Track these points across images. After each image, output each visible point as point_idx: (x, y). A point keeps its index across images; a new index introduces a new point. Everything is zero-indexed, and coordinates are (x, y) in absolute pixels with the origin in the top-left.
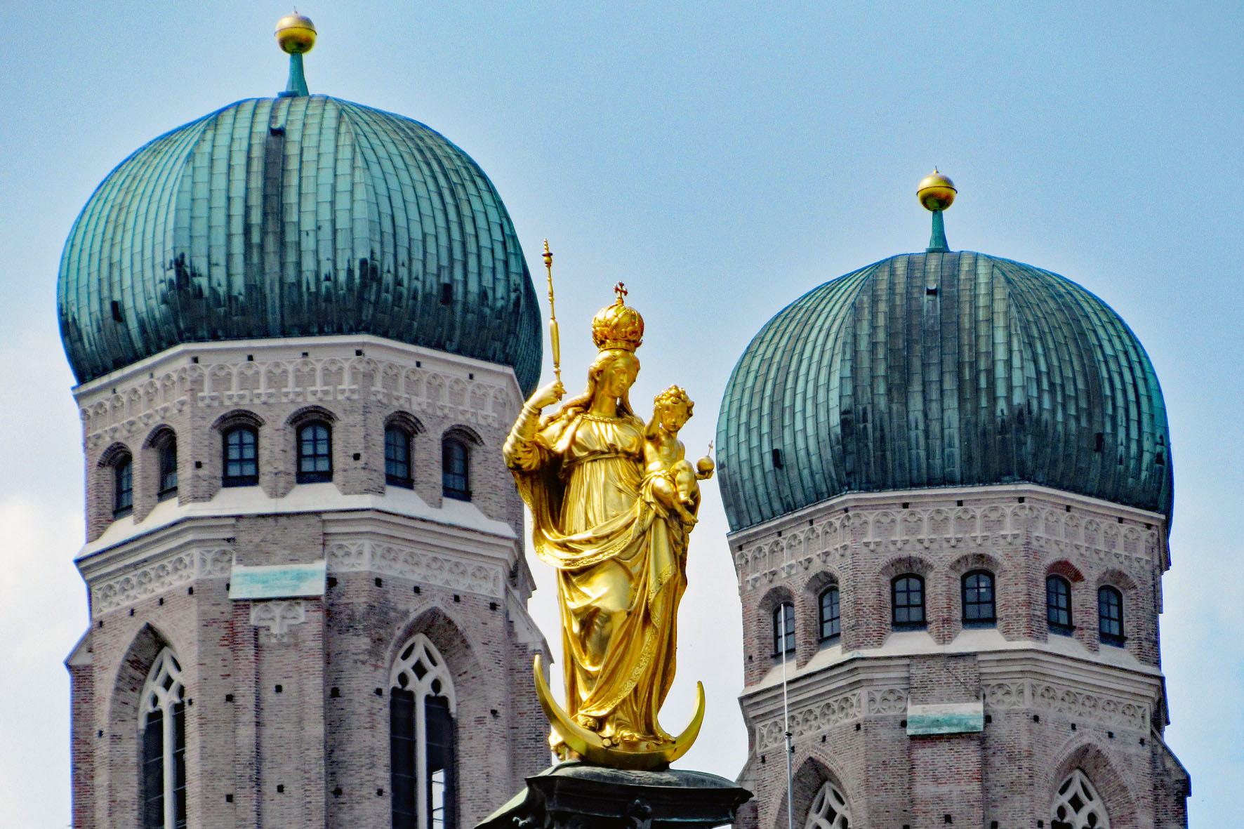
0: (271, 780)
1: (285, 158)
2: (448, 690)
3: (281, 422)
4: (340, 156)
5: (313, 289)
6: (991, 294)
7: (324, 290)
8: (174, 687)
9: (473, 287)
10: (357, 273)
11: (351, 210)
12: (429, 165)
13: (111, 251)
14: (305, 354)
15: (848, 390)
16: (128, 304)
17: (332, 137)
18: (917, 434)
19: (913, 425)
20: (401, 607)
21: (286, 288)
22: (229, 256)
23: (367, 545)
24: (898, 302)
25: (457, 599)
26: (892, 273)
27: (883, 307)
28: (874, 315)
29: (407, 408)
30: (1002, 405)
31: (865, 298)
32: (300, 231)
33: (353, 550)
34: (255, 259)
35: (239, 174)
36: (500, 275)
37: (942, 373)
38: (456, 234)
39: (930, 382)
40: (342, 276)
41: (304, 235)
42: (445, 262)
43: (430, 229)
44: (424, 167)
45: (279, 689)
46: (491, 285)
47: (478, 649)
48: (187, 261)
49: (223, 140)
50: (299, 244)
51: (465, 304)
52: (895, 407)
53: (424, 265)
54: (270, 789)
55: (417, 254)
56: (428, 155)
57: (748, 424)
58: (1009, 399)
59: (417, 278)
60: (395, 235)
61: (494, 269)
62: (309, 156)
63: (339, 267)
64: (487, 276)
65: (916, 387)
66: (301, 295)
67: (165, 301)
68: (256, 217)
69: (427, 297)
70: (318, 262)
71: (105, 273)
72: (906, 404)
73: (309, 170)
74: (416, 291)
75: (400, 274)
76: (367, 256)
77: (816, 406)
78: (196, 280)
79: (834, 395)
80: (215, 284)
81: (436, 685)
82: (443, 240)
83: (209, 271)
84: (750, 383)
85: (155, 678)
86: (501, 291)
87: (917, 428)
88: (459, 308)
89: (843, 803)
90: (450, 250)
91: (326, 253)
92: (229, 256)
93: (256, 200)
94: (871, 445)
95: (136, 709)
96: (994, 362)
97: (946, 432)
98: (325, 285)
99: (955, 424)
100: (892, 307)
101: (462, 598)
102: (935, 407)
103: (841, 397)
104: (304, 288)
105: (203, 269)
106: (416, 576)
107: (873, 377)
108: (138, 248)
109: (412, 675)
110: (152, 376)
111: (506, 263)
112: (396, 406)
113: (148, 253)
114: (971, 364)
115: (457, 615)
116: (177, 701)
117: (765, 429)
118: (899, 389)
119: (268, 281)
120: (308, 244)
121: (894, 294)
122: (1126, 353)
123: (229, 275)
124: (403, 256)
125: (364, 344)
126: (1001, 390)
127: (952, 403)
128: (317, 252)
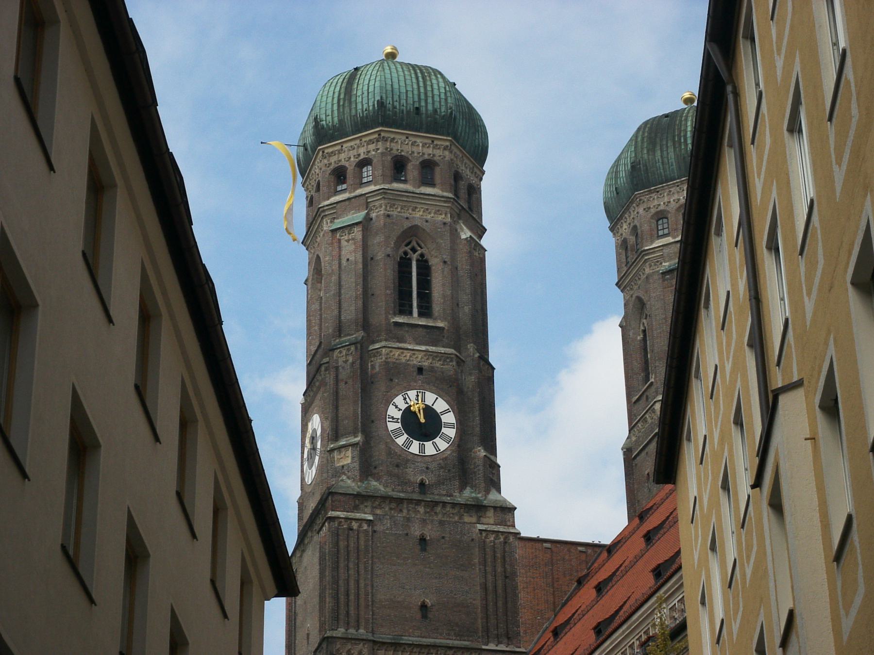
5: (361, 115)
9: (430, 107)
10: (376, 106)
15: (633, 155)
21: (352, 118)
22: (332, 111)
34: (341, 110)
36: (443, 104)
38: (422, 90)
39: (663, 145)
40: (371, 108)
42: (416, 99)
43: (409, 88)
45: (348, 260)
46: (439, 107)
48: (318, 117)
51: (426, 114)
52: (650, 157)
53: (407, 102)
55: (403, 97)
60: (392, 91)
61: (440, 102)
64: (437, 105)
65: (658, 148)
66: (357, 118)
68: (342, 96)
69: (408, 112)
70: (363, 105)
72: (654, 154)
73: (363, 77)
74: (403, 111)
76: (380, 98)
81: (422, 255)
82: (416, 92)
86: (443, 109)
87: (659, 162)
88: (424, 116)
92: (332, 111)
93: (343, 90)
94: (642, 172)
96: (686, 132)
102: (665, 153)
105: (324, 119)
107: (642, 149)
111: (446, 100)
119: (346, 116)
120: (359, 100)
123: (332, 118)
124: (396, 98)
125: (381, 130)
127: (671, 150)
128: (362, 102)
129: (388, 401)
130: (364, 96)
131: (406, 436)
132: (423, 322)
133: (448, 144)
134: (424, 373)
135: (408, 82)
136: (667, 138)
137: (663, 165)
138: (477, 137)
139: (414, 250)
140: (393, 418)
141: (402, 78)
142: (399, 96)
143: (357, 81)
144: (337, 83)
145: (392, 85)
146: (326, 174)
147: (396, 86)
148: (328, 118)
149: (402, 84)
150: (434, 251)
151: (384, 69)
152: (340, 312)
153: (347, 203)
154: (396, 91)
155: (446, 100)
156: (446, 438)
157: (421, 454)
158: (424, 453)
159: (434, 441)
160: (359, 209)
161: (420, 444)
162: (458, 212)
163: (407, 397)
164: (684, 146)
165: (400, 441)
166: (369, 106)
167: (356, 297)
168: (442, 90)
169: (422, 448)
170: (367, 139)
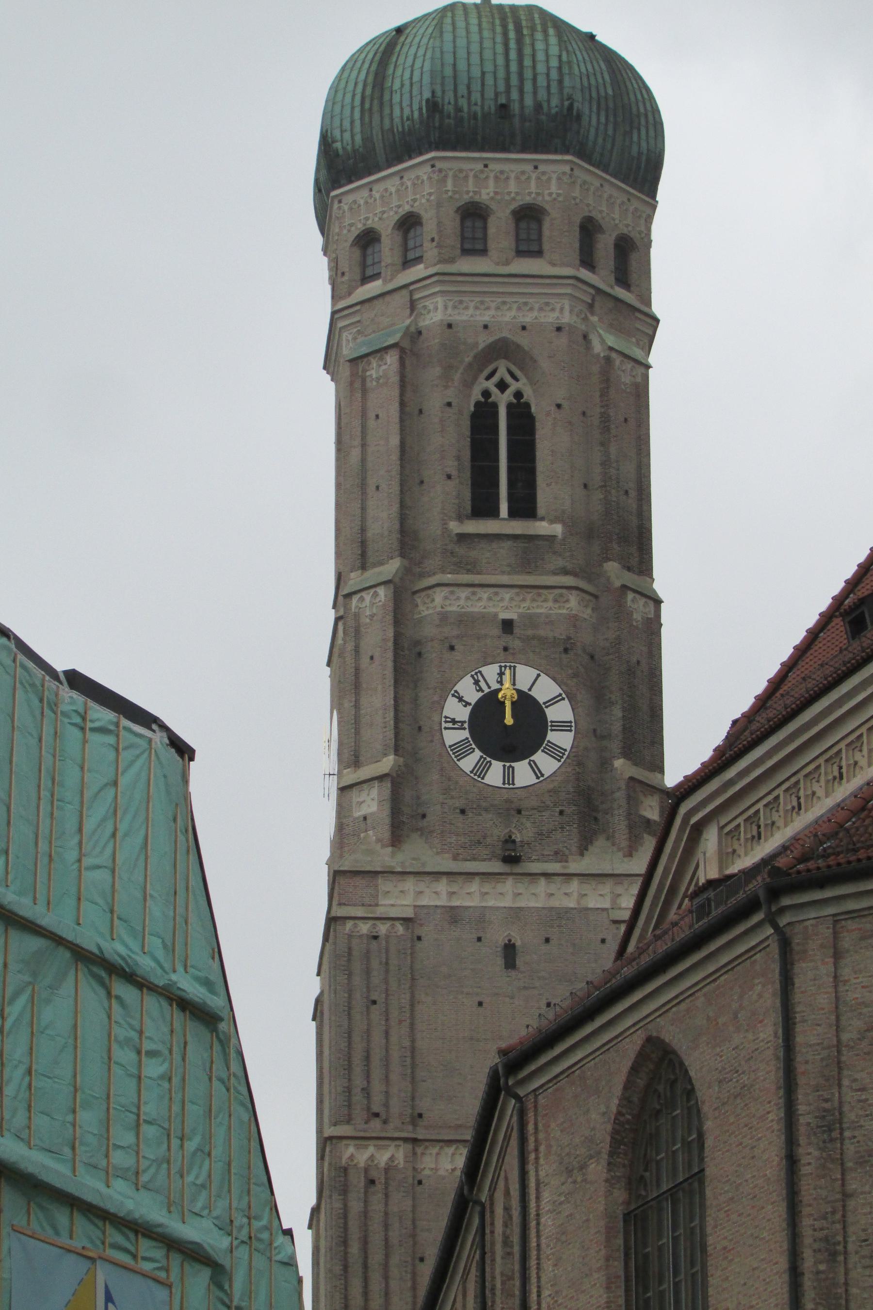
0: (372, 482)
2: (529, 394)
3: (389, 230)
5: (400, 129)
9: (529, 101)
12: (505, 27)
14: (402, 178)
20: (470, 341)
22: (352, 122)
23: (440, 300)
25: (524, 328)
29: (477, 198)
33: (431, 307)
34: (367, 119)
36: (554, 89)
38: (514, 67)
40: (416, 115)
42: (501, 88)
43: (489, 67)
45: (377, 416)
46: (545, 98)
47: (544, 364)
48: (329, 134)
50: (391, 100)
53: (482, 95)
54: (371, 489)
55: (476, 87)
59: (476, 104)
60: (455, 77)
61: (548, 87)
64: (542, 94)
68: (369, 91)
69: (486, 116)
70: (402, 109)
74: (475, 114)
75: (460, 104)
78: (335, 145)
81: (518, 395)
82: (501, 74)
83: (342, 136)
86: (555, 102)
90: (507, 79)
101: (528, 327)
105: (338, 137)
106: (486, 317)
109: (495, 391)
111: (560, 82)
112: (466, 198)
115: (523, 340)
119: (374, 132)
120: (396, 98)
123: (352, 136)
124: (462, 90)
125: (433, 159)
129: (446, 688)
131: (478, 754)
132: (518, 527)
133: (567, 168)
134: (516, 631)
135: (488, 54)
138: (635, 138)
139: (502, 386)
140: (454, 721)
141: (475, 48)
142: (468, 87)
143: (394, 59)
144: (363, 62)
145: (455, 65)
147: (462, 66)
149: (475, 59)
151: (441, 33)
154: (463, 79)
155: (560, 82)
156: (555, 752)
157: (507, 786)
158: (513, 784)
159: (532, 758)
161: (504, 766)
162: (590, 301)
163: (480, 678)
165: (468, 763)
166: (412, 111)
168: (554, 63)
169: (509, 776)
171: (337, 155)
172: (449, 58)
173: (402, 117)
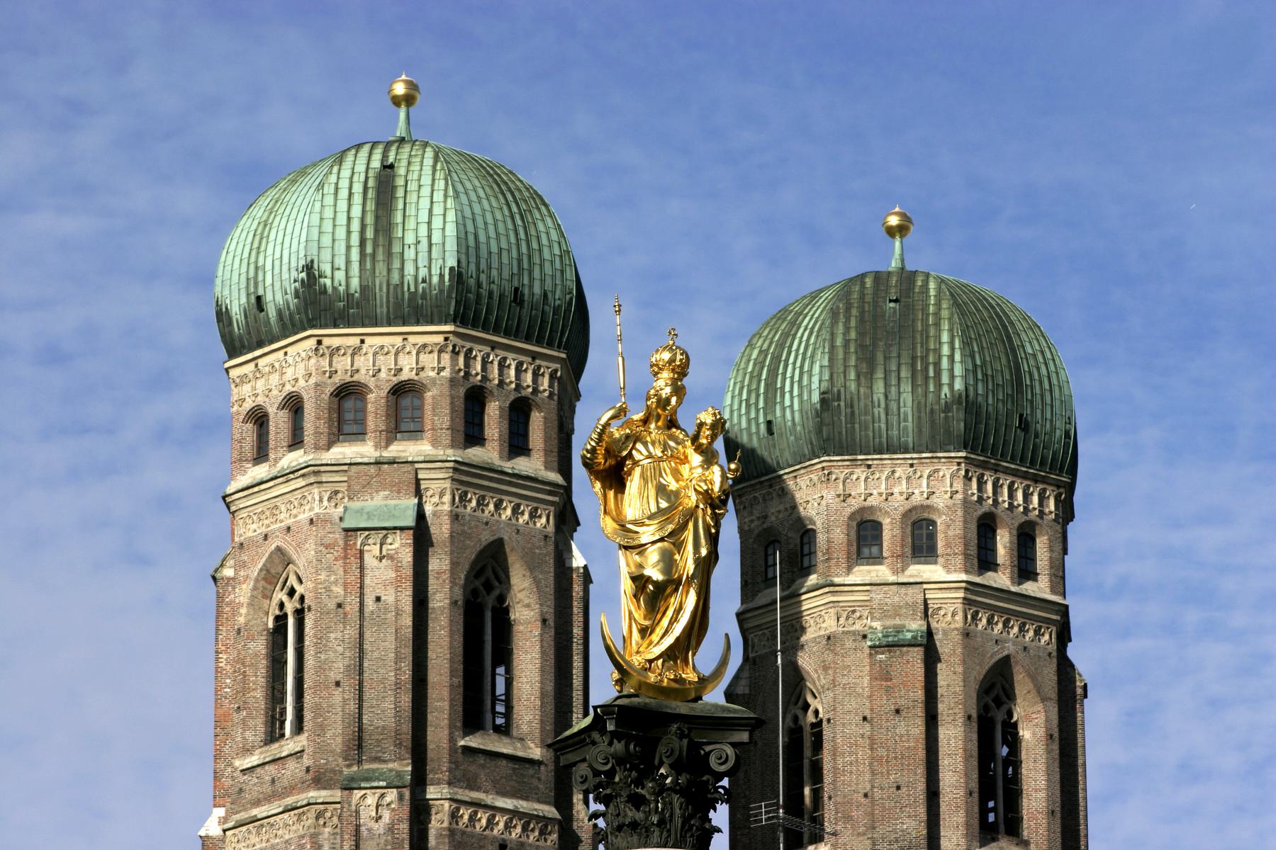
1: (394, 188)
4: (436, 188)
5: (412, 289)
6: (938, 304)
7: (421, 290)
8: (297, 596)
9: (537, 290)
10: (447, 277)
11: (443, 229)
12: (504, 195)
13: (257, 258)
15: (826, 376)
16: (269, 297)
17: (430, 172)
18: (880, 411)
19: (876, 404)
21: (392, 288)
22: (348, 262)
24: (867, 309)
26: (863, 284)
27: (854, 312)
28: (848, 319)
30: (945, 390)
31: (841, 306)
32: (403, 245)
34: (368, 266)
35: (358, 199)
37: (899, 365)
38: (524, 249)
39: (890, 371)
40: (435, 280)
41: (406, 247)
43: (504, 245)
44: (500, 196)
45: (378, 599)
48: (316, 266)
49: (346, 173)
50: (402, 254)
52: (862, 390)
55: (495, 264)
56: (504, 188)
57: (747, 400)
58: (951, 385)
62: (412, 186)
63: (433, 272)
64: (548, 282)
65: (879, 374)
66: (403, 293)
67: (297, 295)
68: (370, 234)
70: (417, 268)
71: (252, 274)
73: (412, 198)
76: (455, 264)
77: (800, 387)
79: (815, 379)
80: (336, 283)
84: (750, 369)
85: (282, 590)
87: (879, 406)
89: (816, 697)
90: (520, 261)
91: (422, 261)
92: (348, 262)
93: (370, 219)
94: (843, 418)
95: (267, 613)
96: (940, 357)
97: (902, 410)
98: (421, 286)
99: (909, 403)
100: (862, 312)
102: (893, 389)
103: (820, 381)
104: (406, 289)
105: (328, 273)
108: (277, 255)
110: (286, 354)
113: (285, 260)
114: (922, 358)
116: (299, 606)
117: (761, 405)
118: (866, 375)
120: (410, 254)
121: (864, 302)
122: (1042, 352)
123: (348, 277)
126: (945, 379)
127: (906, 387)
128: (416, 260)
130: (420, 247)
136: (899, 356)
137: (887, 414)
141: (490, 220)
143: (400, 206)
146: (323, 392)
147: (482, 238)
148: (337, 273)
150: (524, 592)
152: (360, 708)
153: (373, 469)
160: (399, 492)
164: (935, 386)
167: (398, 685)
170: (421, 340)
171: (324, 290)
172: (470, 228)
173: (416, 277)
